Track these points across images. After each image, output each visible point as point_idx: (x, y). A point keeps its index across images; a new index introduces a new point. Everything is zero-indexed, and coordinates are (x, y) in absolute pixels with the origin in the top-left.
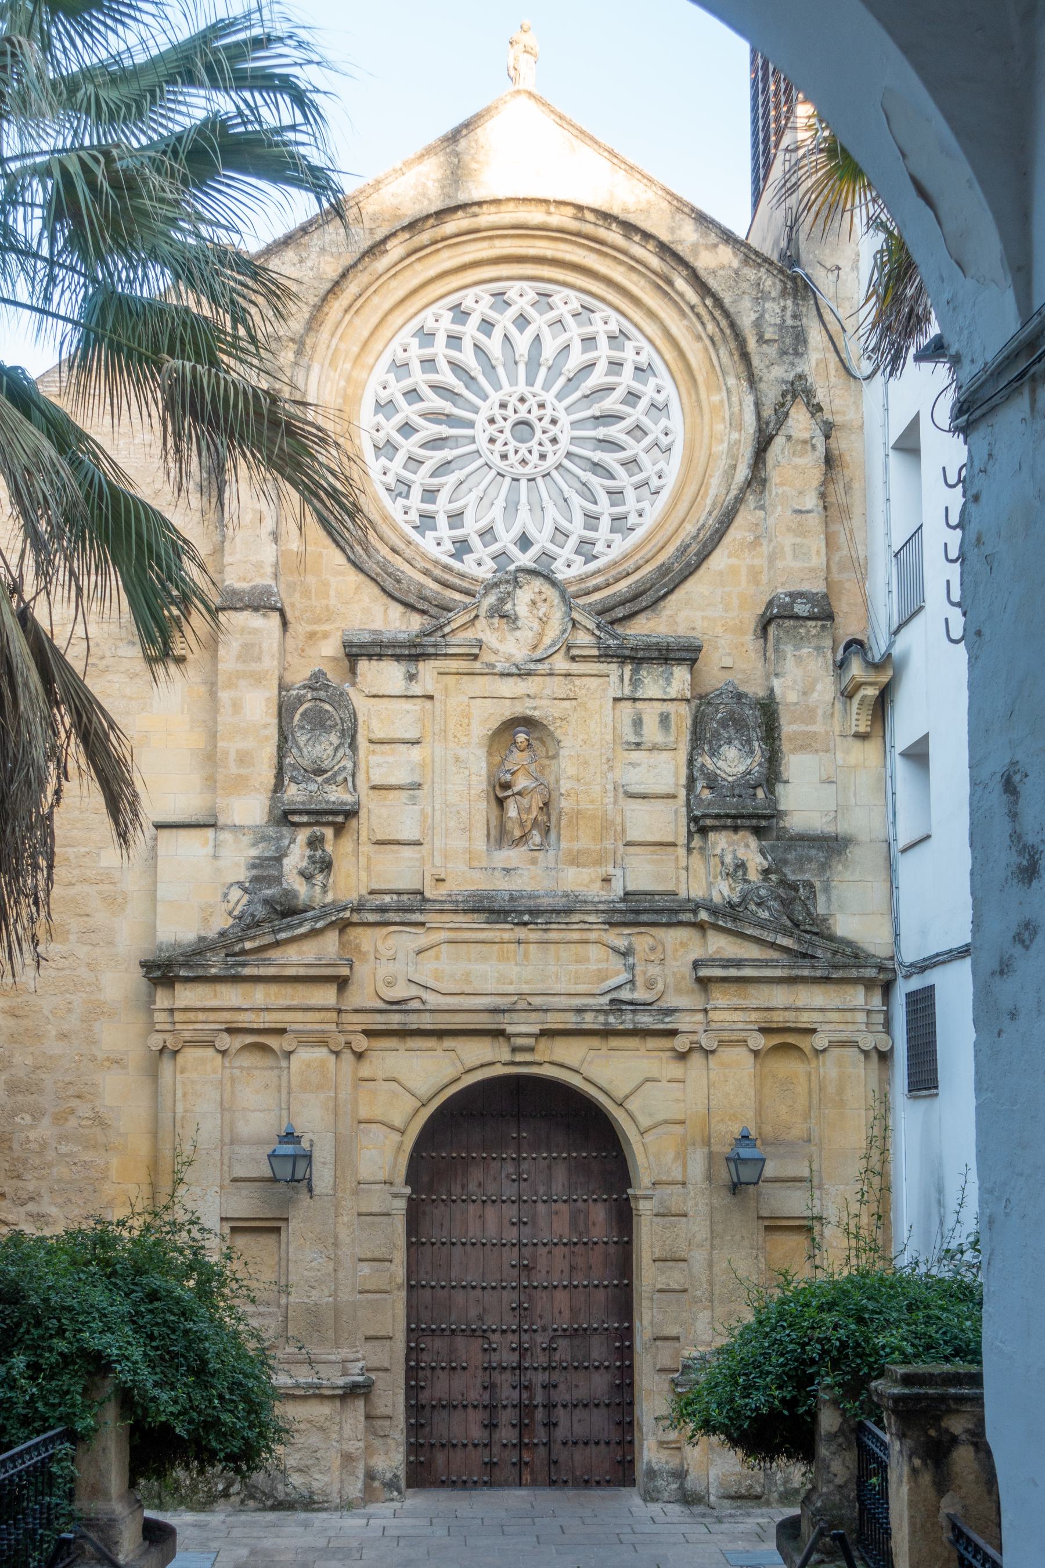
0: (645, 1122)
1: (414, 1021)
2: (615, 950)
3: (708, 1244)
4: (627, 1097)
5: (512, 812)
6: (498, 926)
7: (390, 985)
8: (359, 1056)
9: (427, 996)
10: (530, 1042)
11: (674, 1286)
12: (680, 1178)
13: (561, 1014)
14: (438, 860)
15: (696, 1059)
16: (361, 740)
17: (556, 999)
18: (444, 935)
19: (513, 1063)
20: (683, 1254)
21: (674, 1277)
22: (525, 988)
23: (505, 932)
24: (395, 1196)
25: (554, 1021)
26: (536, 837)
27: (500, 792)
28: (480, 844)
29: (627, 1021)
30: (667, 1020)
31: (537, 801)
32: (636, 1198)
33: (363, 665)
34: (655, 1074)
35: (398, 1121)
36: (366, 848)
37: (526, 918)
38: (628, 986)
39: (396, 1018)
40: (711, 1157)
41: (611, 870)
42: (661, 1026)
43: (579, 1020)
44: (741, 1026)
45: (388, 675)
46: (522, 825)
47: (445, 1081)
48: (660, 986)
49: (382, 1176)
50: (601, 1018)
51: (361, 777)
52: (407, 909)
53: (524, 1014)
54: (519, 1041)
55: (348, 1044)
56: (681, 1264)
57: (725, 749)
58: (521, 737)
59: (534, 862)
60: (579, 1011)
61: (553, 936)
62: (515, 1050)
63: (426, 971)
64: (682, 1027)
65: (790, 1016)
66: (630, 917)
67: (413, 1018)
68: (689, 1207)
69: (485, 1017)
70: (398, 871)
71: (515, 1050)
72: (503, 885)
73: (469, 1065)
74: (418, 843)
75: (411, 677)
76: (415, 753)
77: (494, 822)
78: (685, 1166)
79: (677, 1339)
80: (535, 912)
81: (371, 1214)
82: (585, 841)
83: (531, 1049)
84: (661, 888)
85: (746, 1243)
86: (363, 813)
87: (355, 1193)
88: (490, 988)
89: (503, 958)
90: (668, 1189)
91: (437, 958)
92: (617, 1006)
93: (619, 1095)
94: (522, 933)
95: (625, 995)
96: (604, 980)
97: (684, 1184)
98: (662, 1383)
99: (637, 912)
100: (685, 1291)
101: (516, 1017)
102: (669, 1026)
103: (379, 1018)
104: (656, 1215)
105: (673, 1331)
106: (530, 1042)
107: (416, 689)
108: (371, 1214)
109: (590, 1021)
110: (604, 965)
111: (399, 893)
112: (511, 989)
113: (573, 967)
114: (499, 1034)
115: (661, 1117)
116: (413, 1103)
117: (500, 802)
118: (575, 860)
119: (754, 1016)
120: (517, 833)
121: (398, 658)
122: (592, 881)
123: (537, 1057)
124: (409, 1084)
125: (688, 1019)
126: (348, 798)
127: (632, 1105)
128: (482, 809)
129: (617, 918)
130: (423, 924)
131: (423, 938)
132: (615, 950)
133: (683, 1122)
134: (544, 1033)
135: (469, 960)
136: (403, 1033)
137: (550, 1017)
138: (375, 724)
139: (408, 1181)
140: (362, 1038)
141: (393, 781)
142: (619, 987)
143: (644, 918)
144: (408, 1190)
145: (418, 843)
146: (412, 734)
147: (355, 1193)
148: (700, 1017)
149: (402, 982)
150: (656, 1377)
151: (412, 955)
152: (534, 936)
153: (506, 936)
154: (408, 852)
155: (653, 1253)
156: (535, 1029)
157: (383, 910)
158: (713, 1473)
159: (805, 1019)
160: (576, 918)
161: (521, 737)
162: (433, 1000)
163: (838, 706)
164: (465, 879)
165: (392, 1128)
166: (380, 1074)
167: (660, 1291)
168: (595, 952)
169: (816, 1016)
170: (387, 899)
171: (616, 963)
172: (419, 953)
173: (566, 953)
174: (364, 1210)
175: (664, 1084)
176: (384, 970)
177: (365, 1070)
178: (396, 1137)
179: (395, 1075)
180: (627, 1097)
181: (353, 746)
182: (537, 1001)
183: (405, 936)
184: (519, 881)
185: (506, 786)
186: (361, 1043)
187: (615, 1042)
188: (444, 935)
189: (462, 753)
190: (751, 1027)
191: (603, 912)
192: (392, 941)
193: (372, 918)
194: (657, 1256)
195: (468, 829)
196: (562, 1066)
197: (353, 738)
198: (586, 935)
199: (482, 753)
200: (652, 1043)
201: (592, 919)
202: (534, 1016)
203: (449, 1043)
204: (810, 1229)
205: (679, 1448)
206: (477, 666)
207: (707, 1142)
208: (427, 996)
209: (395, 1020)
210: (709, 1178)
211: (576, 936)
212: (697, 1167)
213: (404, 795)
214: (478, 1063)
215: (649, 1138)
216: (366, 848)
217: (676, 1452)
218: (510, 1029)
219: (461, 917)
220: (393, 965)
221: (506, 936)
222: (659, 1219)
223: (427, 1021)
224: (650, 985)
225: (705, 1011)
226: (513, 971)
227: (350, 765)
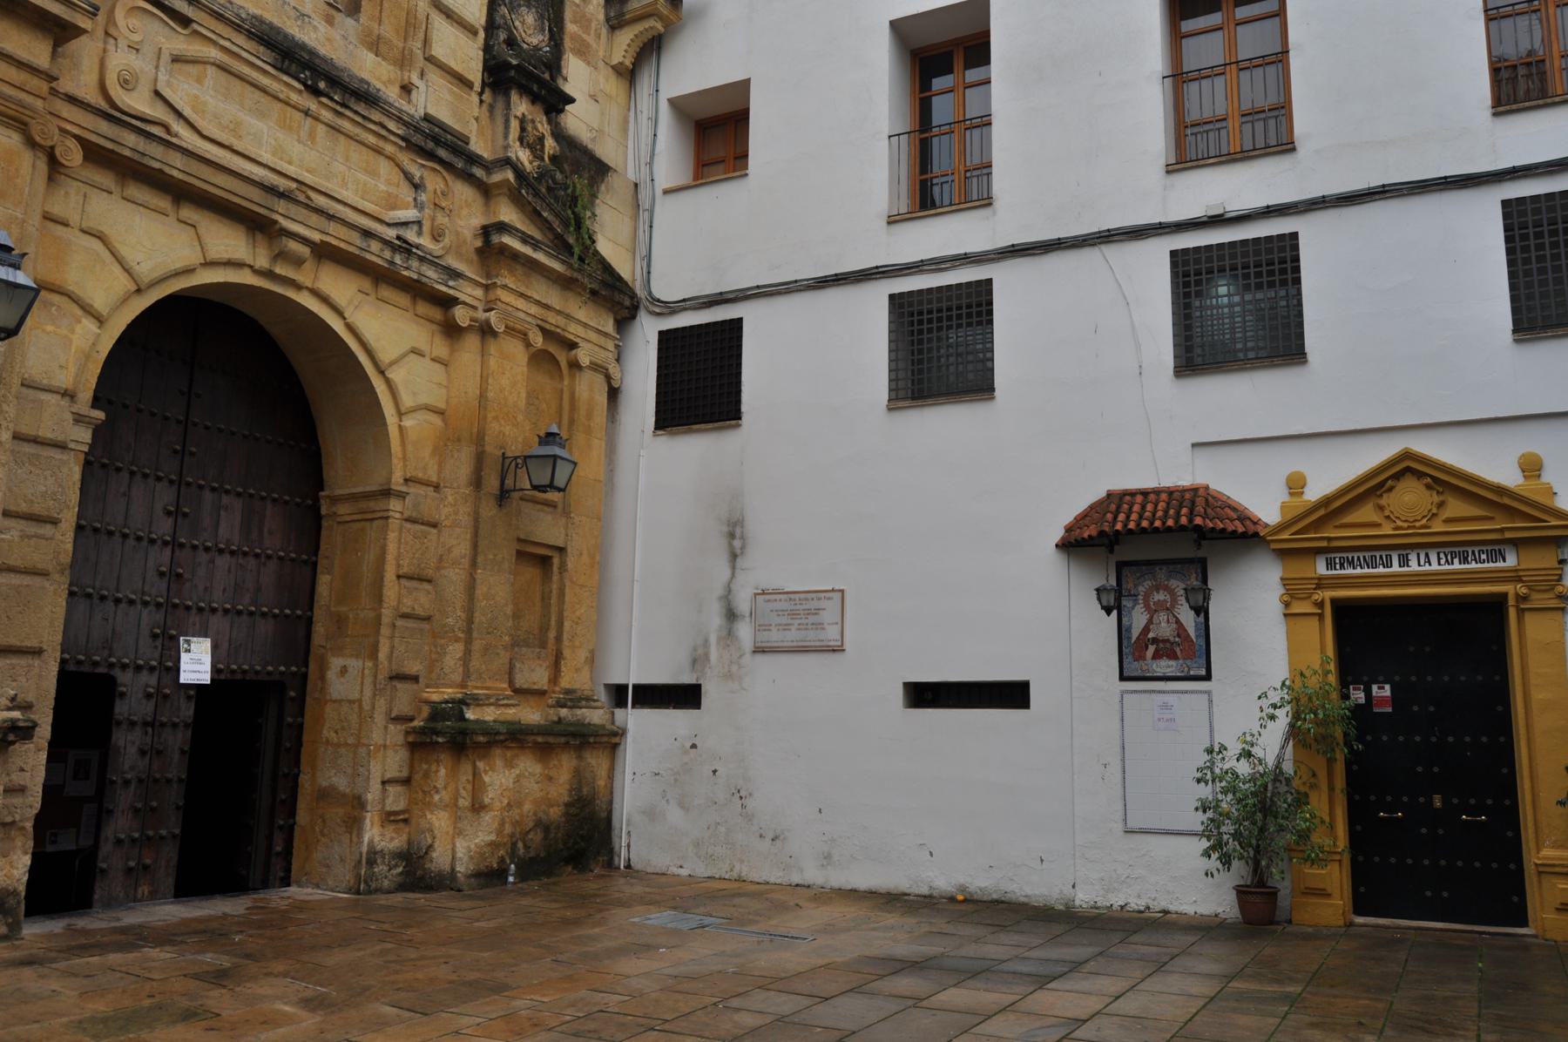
0: (407, 401)
1: (156, 156)
2: (408, 177)
3: (466, 562)
4: (392, 364)
6: (285, 78)
7: (125, 84)
9: (177, 127)
10: (305, 251)
11: (419, 611)
12: (434, 479)
13: (345, 229)
15: (472, 342)
17: (340, 207)
18: (214, 53)
19: (269, 274)
20: (430, 573)
21: (420, 600)
22: (308, 178)
24: (79, 419)
25: (339, 236)
29: (412, 270)
30: (451, 283)
32: (335, 500)
34: (423, 345)
35: (100, 302)
37: (322, 85)
38: (415, 228)
40: (480, 459)
41: (415, 79)
42: (444, 289)
43: (364, 245)
44: (522, 315)
47: (179, 265)
48: (447, 241)
49: (64, 380)
50: (387, 254)
53: (304, 211)
54: (293, 246)
56: (426, 586)
57: (524, 10)
60: (367, 234)
61: (346, 125)
62: (281, 256)
63: (182, 91)
64: (462, 297)
65: (560, 321)
66: (430, 145)
68: (444, 513)
69: (255, 194)
78: (440, 465)
79: (415, 679)
81: (35, 441)
82: (388, 30)
83: (298, 262)
84: (457, 127)
85: (506, 565)
88: (266, 157)
89: (285, 125)
90: (421, 490)
91: (199, 80)
92: (406, 248)
93: (385, 357)
94: (312, 104)
95: (411, 235)
96: (393, 208)
97: (437, 487)
98: (396, 733)
99: (437, 140)
100: (428, 619)
101: (294, 210)
102: (451, 292)
104: (406, 520)
105: (414, 667)
108: (35, 441)
109: (376, 254)
110: (392, 190)
112: (291, 170)
113: (362, 177)
114: (258, 226)
115: (424, 399)
118: (375, 45)
119: (534, 309)
122: (390, 81)
124: (124, 251)
125: (469, 290)
127: (395, 375)
129: (417, 139)
130: (185, 21)
132: (408, 177)
133: (441, 413)
135: (242, 105)
137: (333, 228)
139: (96, 402)
142: (405, 224)
143: (442, 153)
144: (100, 415)
148: (479, 293)
150: (391, 727)
151: (166, 58)
152: (326, 115)
153: (294, 97)
155: (399, 566)
156: (316, 237)
158: (462, 847)
159: (573, 331)
160: (376, 116)
162: (187, 138)
163: (604, 31)
165: (88, 310)
167: (405, 616)
168: (384, 167)
169: (580, 331)
171: (406, 193)
172: (176, 59)
173: (358, 155)
174: (25, 430)
175: (427, 360)
176: (119, 59)
177: (67, 202)
178: (89, 325)
179: (105, 229)
180: (392, 364)
182: (321, 201)
183: (156, 26)
184: (313, 36)
186: (73, 156)
187: (386, 292)
188: (214, 53)
190: (529, 319)
191: (406, 124)
194: (405, 570)
196: (325, 300)
198: (381, 144)
200: (423, 308)
201: (392, 126)
202: (314, 219)
203: (188, 213)
204: (544, 562)
205: (405, 821)
207: (479, 439)
208: (177, 127)
210: (477, 482)
211: (372, 139)
212: (460, 466)
214: (226, 256)
215: (408, 422)
217: (401, 825)
219: (241, 40)
221: (294, 97)
222: (408, 525)
223: (176, 167)
224: (436, 236)
225: (487, 288)
226: (296, 149)
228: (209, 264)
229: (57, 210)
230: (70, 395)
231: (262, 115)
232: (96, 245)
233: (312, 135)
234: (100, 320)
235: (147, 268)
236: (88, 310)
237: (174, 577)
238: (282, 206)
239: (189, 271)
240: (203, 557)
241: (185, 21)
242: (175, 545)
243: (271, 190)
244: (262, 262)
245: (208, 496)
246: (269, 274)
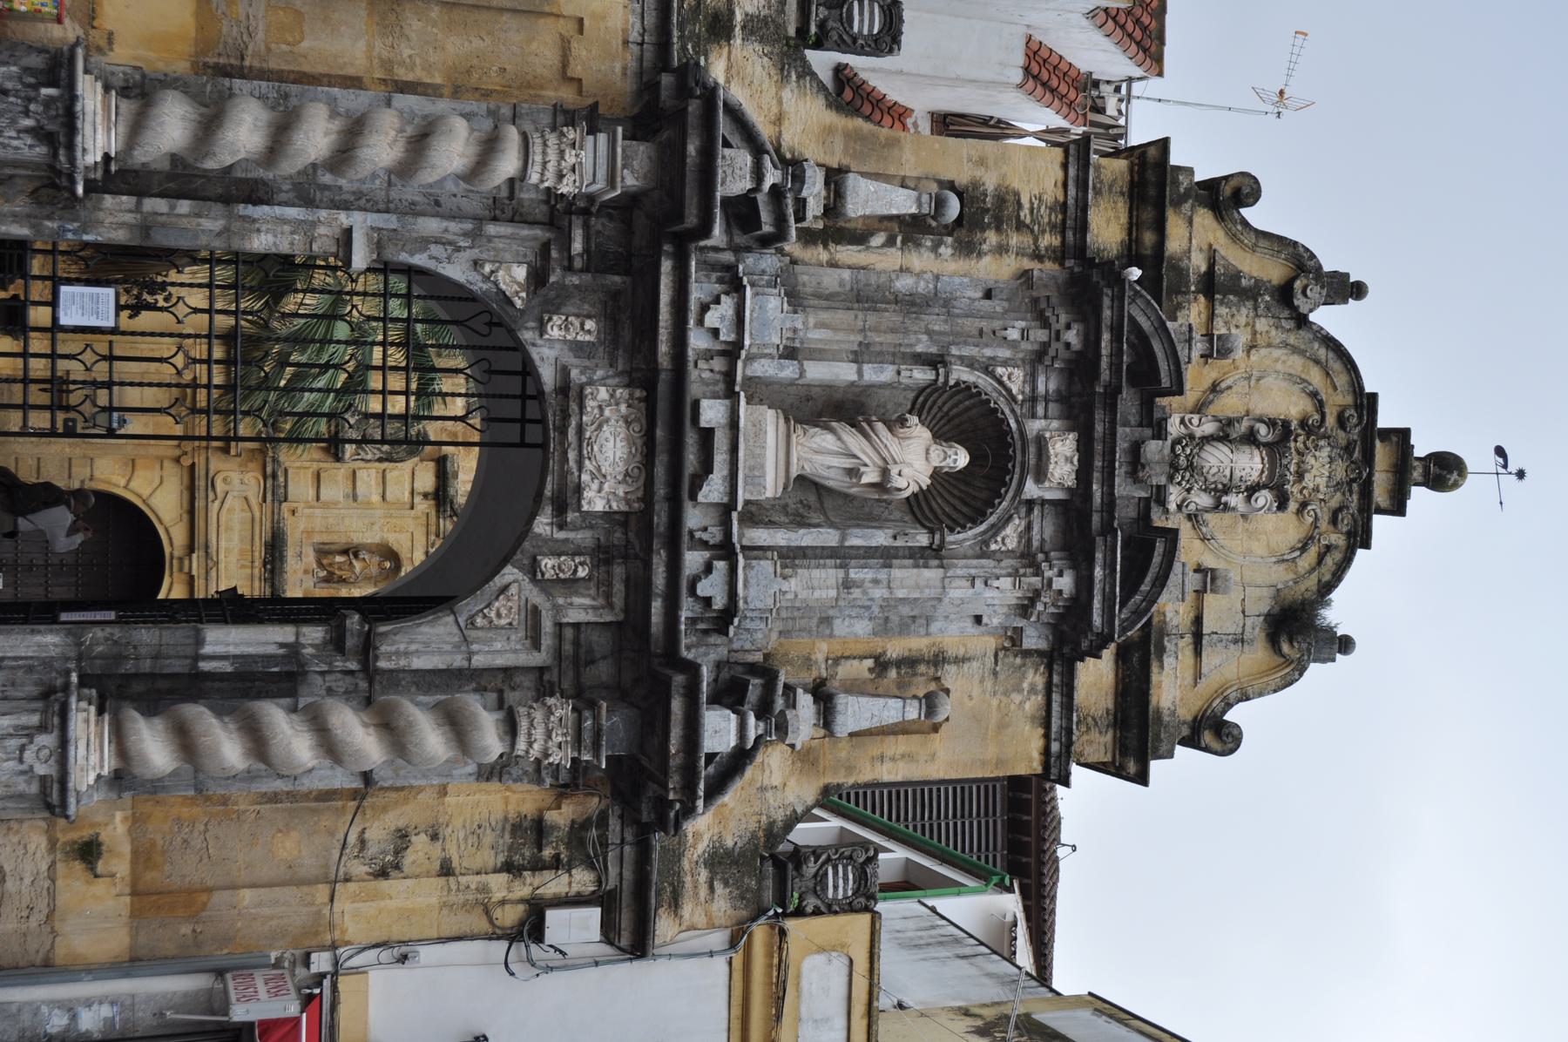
1: (200, 495)
5: (339, 559)
7: (225, 480)
8: (177, 460)
9: (217, 503)
10: (186, 569)
14: (307, 511)
16: (386, 465)
18: (257, 515)
19: (172, 558)
22: (222, 566)
23: (259, 552)
26: (323, 574)
27: (351, 551)
28: (317, 539)
31: (345, 574)
33: (431, 465)
35: (133, 485)
36: (315, 466)
39: (202, 483)
45: (426, 479)
46: (330, 565)
49: (97, 474)
51: (361, 464)
52: (275, 489)
54: (186, 562)
55: (185, 453)
58: (388, 565)
59: (306, 572)
62: (181, 560)
67: (202, 494)
70: (300, 487)
71: (181, 560)
72: (290, 553)
73: (171, 530)
74: (318, 499)
75: (426, 496)
76: (376, 498)
77: (333, 547)
80: (272, 571)
83: (181, 569)
86: (338, 465)
87: (85, 456)
88: (223, 544)
89: (242, 552)
94: (258, 563)
101: (203, 560)
103: (203, 473)
106: (186, 569)
107: (418, 499)
111: (286, 487)
112: (222, 557)
114: (191, 549)
116: (145, 493)
117: (345, 552)
120: (325, 562)
121: (437, 490)
123: (175, 574)
126: (347, 455)
128: (340, 540)
130: (264, 500)
131: (254, 502)
134: (192, 578)
136: (192, 489)
137: (202, 581)
138: (396, 473)
140: (189, 462)
141: (359, 484)
145: (318, 499)
146: (389, 496)
147: (85, 456)
149: (227, 488)
152: (256, 571)
153: (257, 554)
154: (311, 493)
156: (194, 572)
157: (274, 476)
161: (388, 565)
164: (294, 530)
165: (129, 481)
166: (165, 473)
170: (282, 479)
177: (167, 464)
178: (123, 482)
181: (380, 460)
182: (213, 573)
185: (356, 556)
186: (186, 462)
188: (257, 515)
189: (376, 527)
192: (253, 482)
193: (269, 470)
195: (328, 531)
197: (387, 460)
199: (377, 540)
202: (203, 571)
203: (186, 517)
206: (433, 537)
208: (217, 503)
209: (201, 483)
213: (349, 490)
216: (315, 466)
218: (194, 556)
219: (269, 525)
220: (236, 483)
221: (257, 554)
226: (233, 558)
227: (369, 457)
228: (167, 531)
229: (167, 464)
230: (92, 478)
231: (242, 541)
232: (157, 481)
233: (243, 566)
234: (125, 487)
235: (154, 502)
236: (129, 481)
237: (30, 567)
238: (202, 553)
239: (161, 522)
240: (42, 580)
241: (264, 500)
242: (47, 566)
243: (207, 547)
244: (177, 553)
245: (73, 580)
246: (172, 558)
